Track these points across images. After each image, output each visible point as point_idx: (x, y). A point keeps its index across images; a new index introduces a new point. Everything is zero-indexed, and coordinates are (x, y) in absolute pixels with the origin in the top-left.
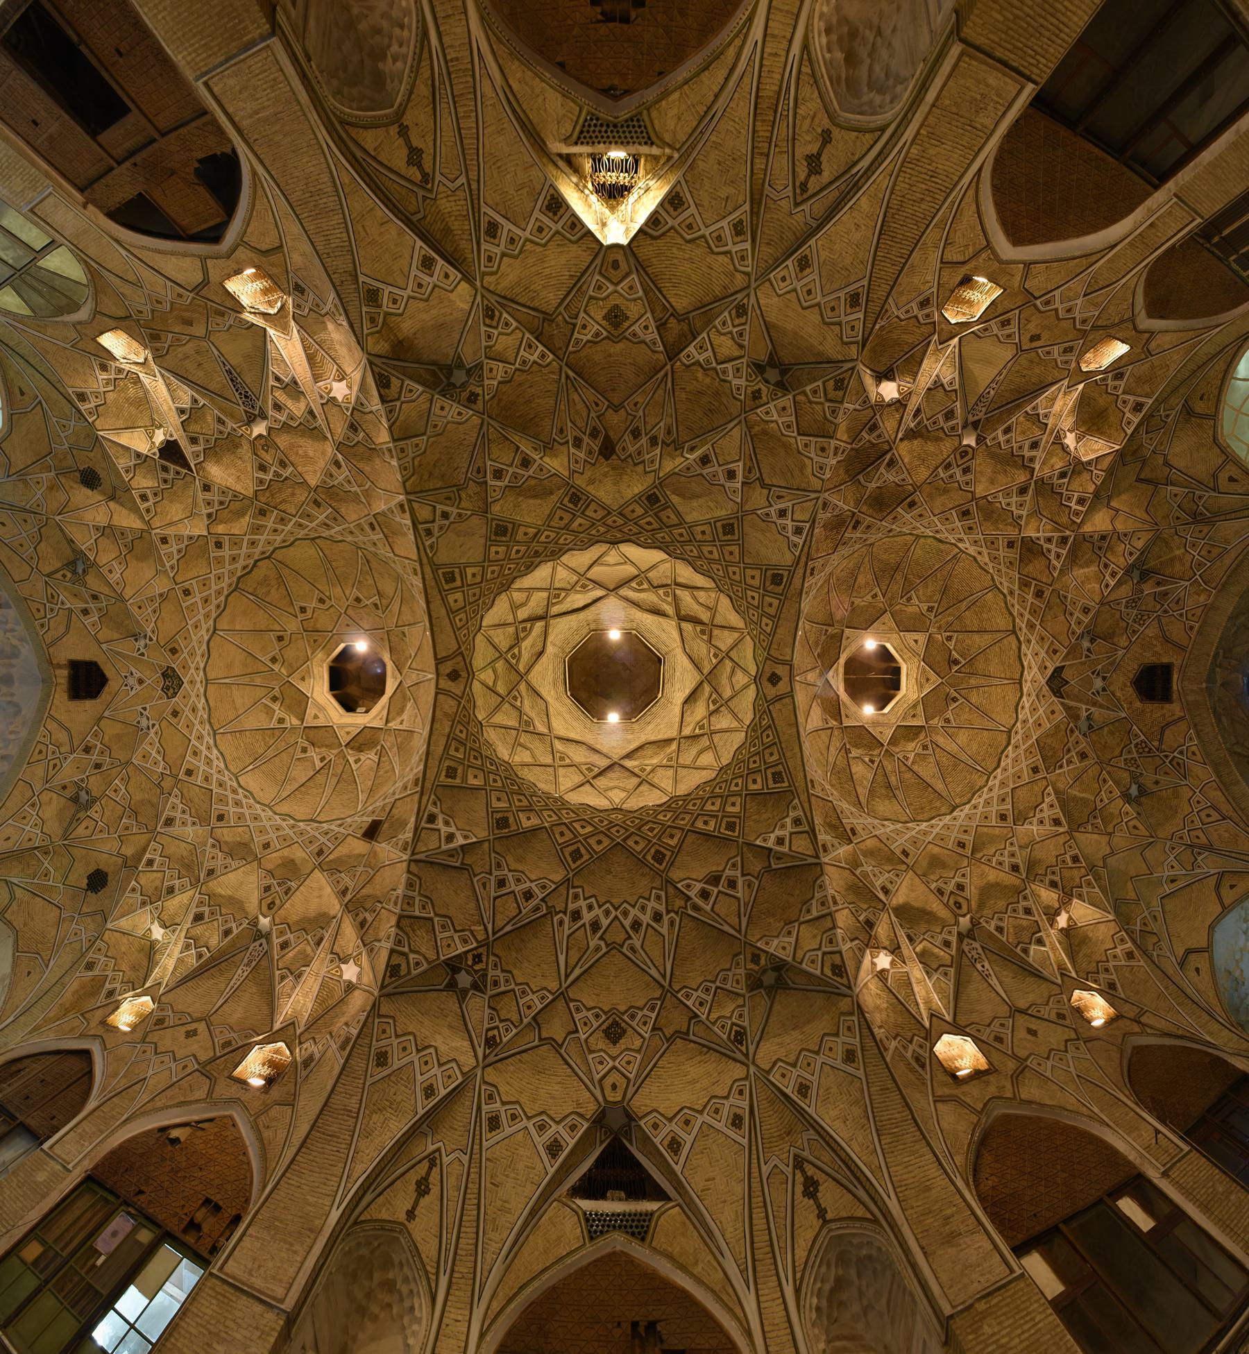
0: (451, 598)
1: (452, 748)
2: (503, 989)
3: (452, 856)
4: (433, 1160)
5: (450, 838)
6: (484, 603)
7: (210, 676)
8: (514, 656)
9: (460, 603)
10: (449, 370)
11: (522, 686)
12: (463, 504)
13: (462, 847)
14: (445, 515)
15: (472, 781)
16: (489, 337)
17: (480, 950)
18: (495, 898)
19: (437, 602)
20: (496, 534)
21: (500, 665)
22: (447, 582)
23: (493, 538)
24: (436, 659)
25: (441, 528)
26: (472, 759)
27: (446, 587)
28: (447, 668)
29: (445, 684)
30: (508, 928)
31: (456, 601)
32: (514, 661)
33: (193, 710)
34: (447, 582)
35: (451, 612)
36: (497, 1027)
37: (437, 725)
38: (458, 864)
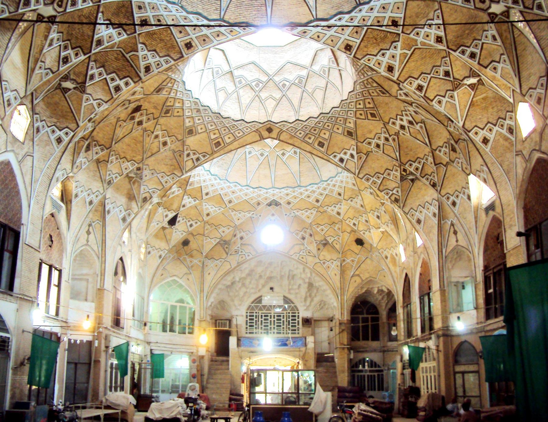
0: (228, 141)
1: (309, 140)
2: (421, 167)
3: (361, 158)
4: (452, 225)
5: (352, 156)
6: (228, 123)
7: (271, 186)
8: (257, 85)
9: (231, 135)
10: (130, 179)
11: (277, 79)
12: (181, 149)
13: (357, 153)
14: (188, 155)
15: (326, 136)
16: (116, 177)
17: (402, 168)
18: (383, 152)
19: (231, 147)
20: (192, 133)
21: (263, 95)
22: (220, 145)
23: (194, 134)
24: (261, 140)
25: (194, 154)
26: (316, 132)
27: (223, 145)
28: (265, 134)
29: (274, 134)
30: (398, 154)
31: (229, 138)
32: (261, 85)
33: (287, 195)
34: (220, 145)
35: (235, 140)
36: (431, 179)
37: (296, 144)
38: (365, 157)
